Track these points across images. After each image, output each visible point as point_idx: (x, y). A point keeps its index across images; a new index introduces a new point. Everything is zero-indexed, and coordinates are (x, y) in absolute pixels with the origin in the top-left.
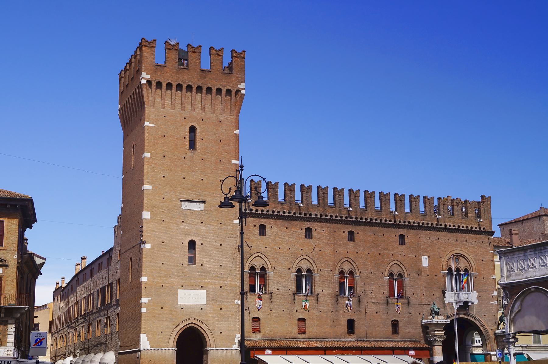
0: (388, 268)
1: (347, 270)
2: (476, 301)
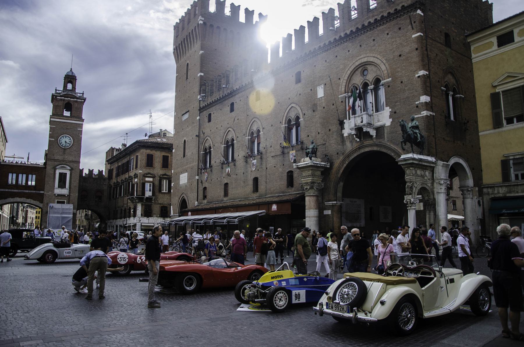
1: (255, 129)
2: (388, 122)
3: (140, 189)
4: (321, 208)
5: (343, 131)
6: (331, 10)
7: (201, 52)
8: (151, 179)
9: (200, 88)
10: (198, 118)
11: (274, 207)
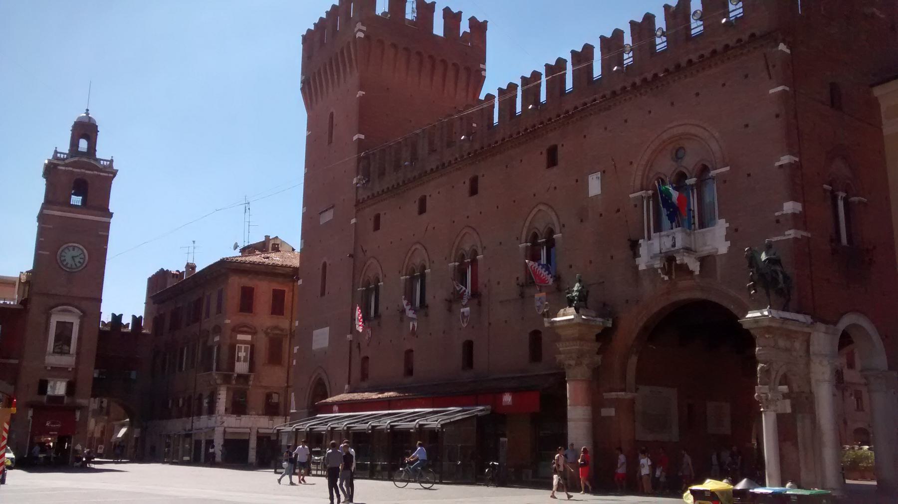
0: (527, 224)
1: (467, 249)
2: (723, 247)
3: (225, 356)
4: (596, 403)
5: (638, 260)
6: (618, 34)
7: (361, 93)
8: (248, 338)
9: (359, 163)
10: (353, 221)
11: (507, 399)
